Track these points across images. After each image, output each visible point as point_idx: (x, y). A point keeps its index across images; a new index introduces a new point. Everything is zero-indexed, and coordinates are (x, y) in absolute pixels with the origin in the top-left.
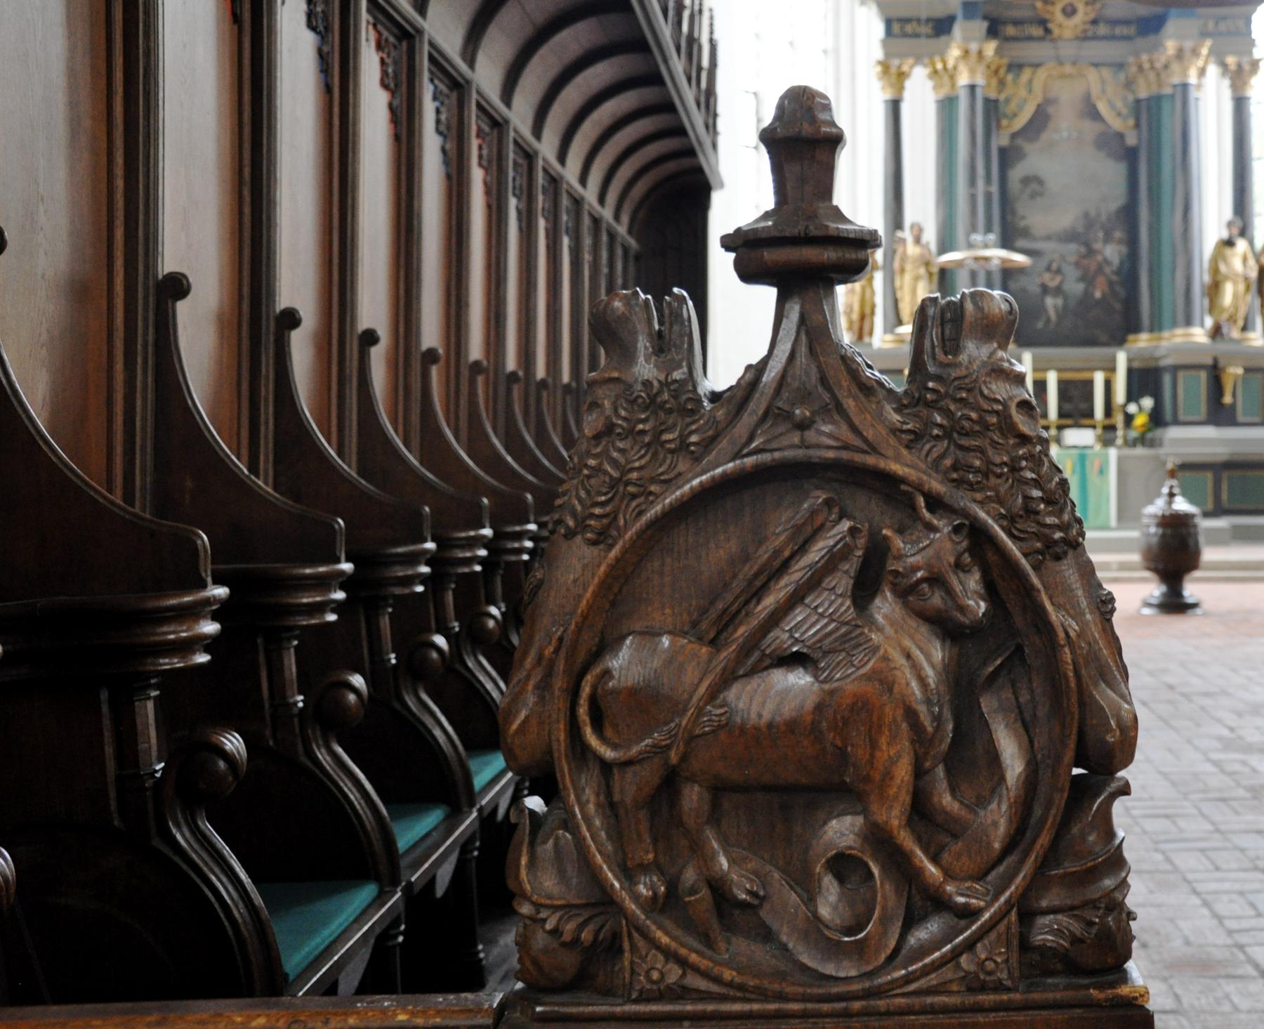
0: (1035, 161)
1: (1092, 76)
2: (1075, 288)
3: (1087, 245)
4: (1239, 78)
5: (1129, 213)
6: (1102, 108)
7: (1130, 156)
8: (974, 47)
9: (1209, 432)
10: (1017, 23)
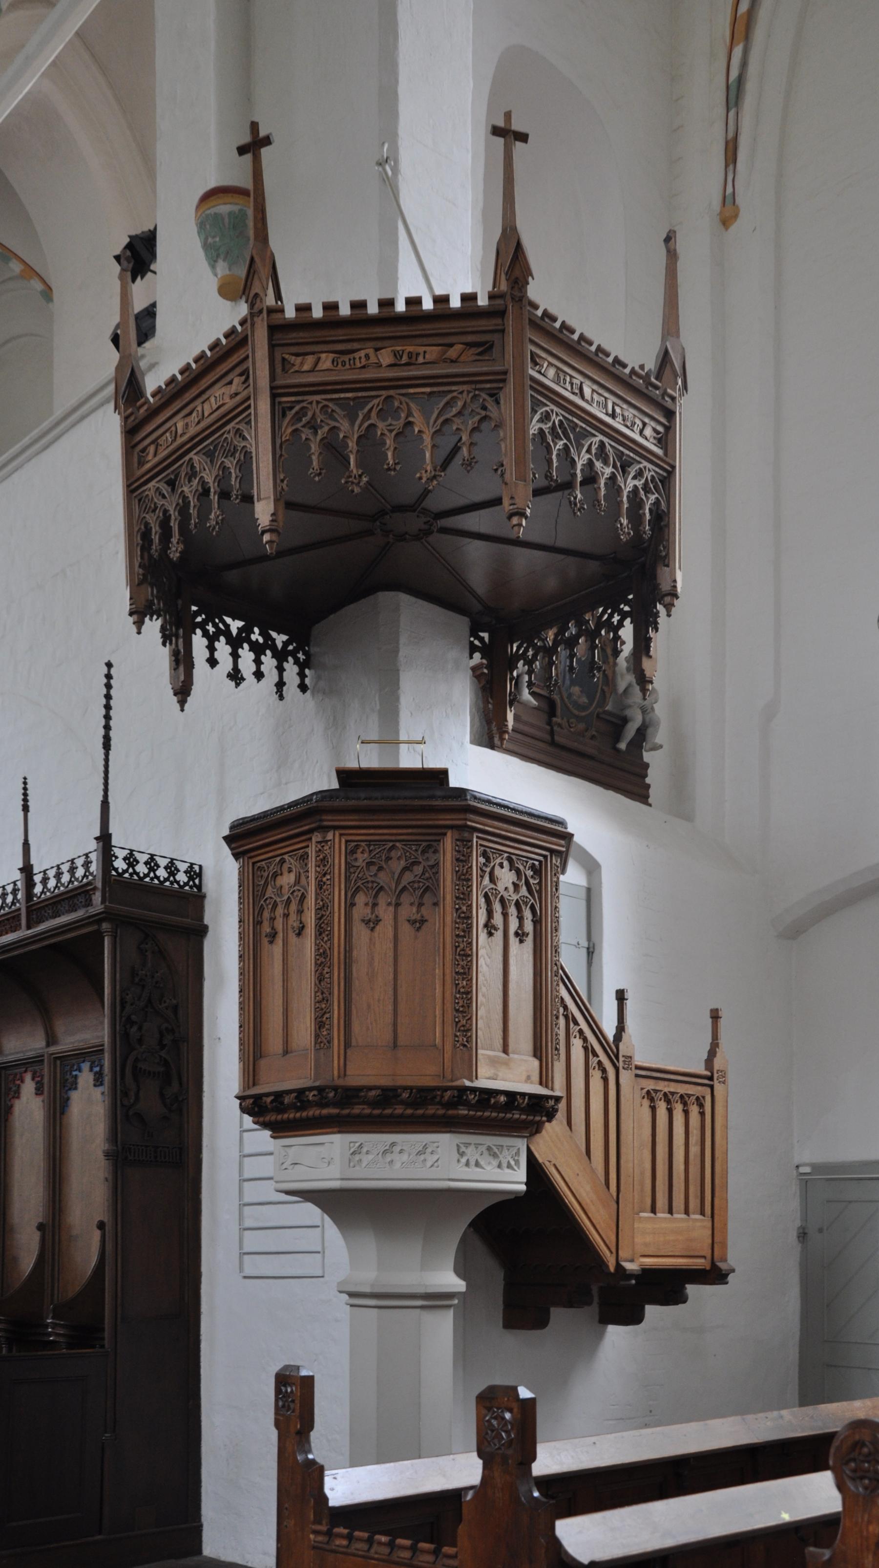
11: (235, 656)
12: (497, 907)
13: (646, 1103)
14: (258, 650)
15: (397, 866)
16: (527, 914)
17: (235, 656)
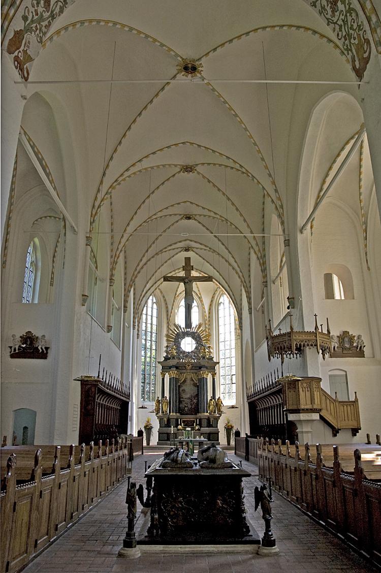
2: (190, 406)
4: (214, 375)
5: (197, 395)
6: (194, 379)
7: (198, 386)
9: (207, 428)
14: (293, 354)
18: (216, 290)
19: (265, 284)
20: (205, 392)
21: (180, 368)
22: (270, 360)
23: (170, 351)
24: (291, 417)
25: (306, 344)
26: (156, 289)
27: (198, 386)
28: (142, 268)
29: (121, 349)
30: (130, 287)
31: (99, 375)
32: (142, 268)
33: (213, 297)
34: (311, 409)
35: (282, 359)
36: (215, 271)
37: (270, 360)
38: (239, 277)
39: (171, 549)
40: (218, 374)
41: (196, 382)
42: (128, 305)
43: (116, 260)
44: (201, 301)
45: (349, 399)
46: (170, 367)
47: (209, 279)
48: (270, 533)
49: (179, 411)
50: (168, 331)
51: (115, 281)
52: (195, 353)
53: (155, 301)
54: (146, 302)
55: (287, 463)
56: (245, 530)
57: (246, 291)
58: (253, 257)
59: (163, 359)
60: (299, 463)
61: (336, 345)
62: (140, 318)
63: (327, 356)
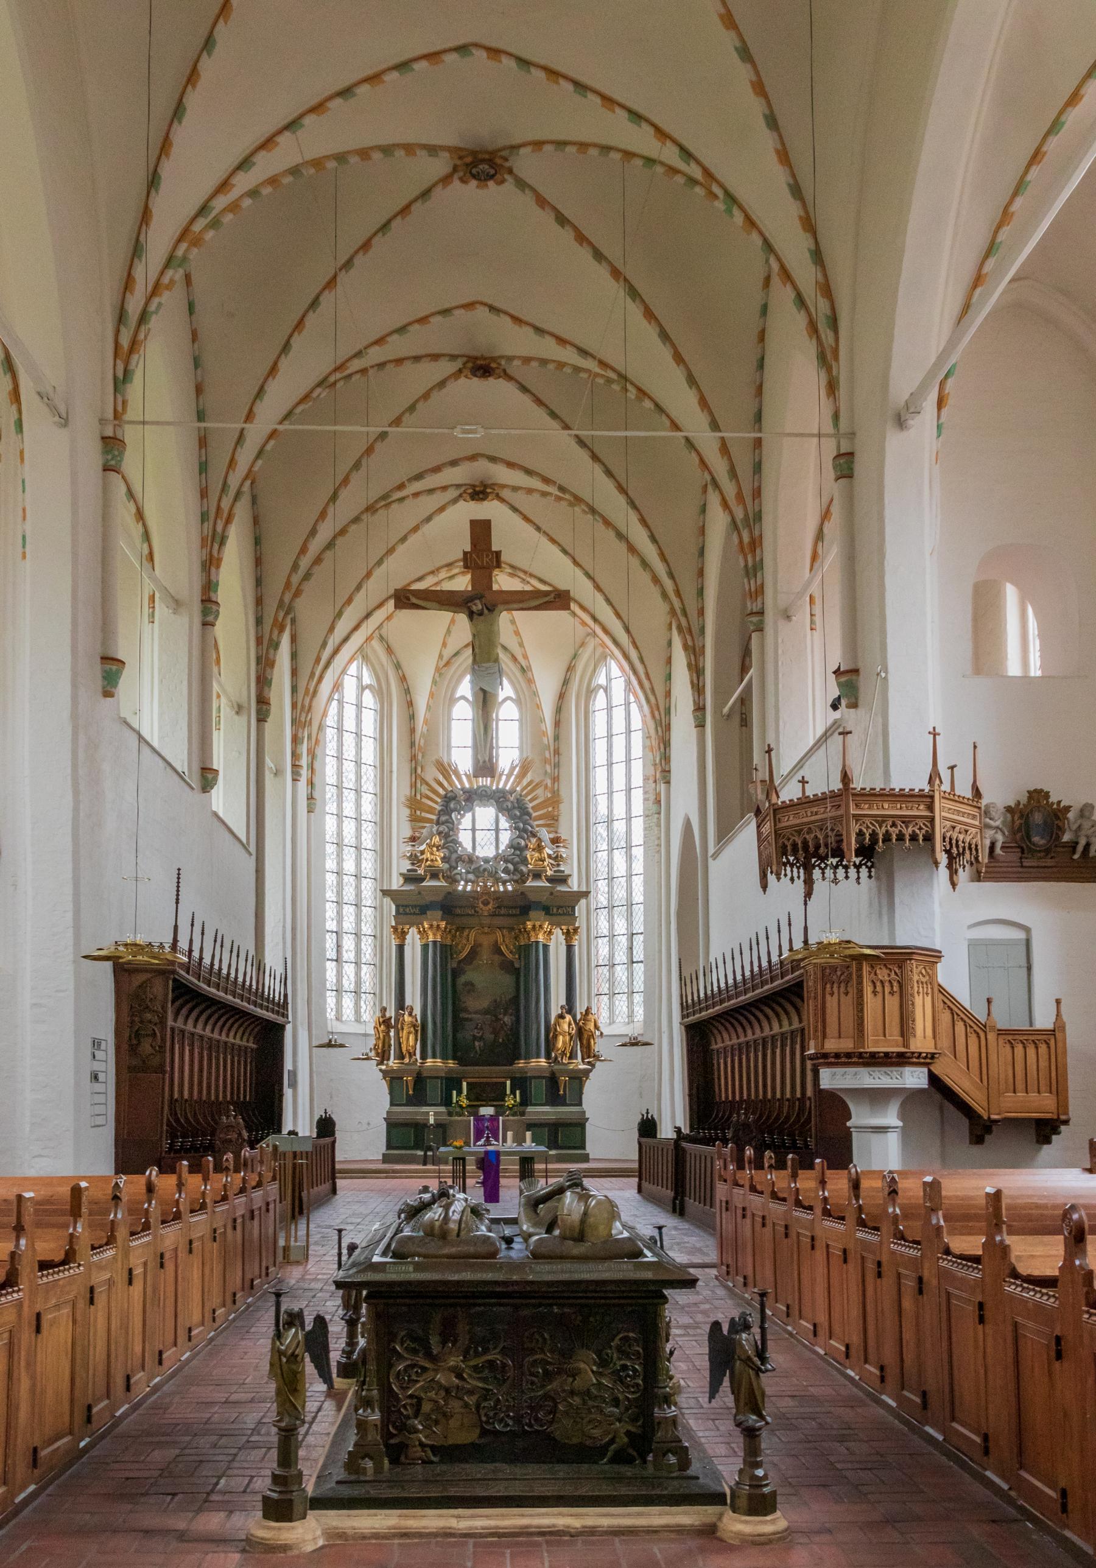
0: (470, 975)
1: (499, 934)
3: (496, 1016)
6: (503, 948)
7: (516, 972)
8: (435, 923)
10: (461, 907)
11: (835, 873)
12: (878, 984)
13: (1008, 1046)
14: (846, 867)
15: (839, 973)
16: (895, 984)
17: (835, 873)
18: (583, 644)
19: (755, 619)
20: (542, 989)
21: (458, 911)
22: (764, 886)
23: (422, 853)
24: (830, 1079)
25: (894, 831)
26: (369, 639)
27: (516, 972)
28: (318, 560)
29: (252, 848)
30: (276, 632)
31: (175, 941)
32: (318, 560)
33: (570, 669)
34: (901, 1055)
35: (809, 883)
36: (579, 573)
37: (764, 886)
38: (665, 595)
39: (424, 1523)
40: (583, 931)
41: (510, 956)
42: (273, 696)
43: (219, 529)
44: (530, 681)
45: (1031, 1025)
46: (423, 910)
47: (558, 600)
48: (760, 1473)
49: (455, 1051)
50: (414, 786)
51: (221, 610)
52: (506, 861)
53: (367, 679)
54: (337, 686)
55: (818, 1233)
56: (672, 1459)
57: (686, 647)
58: (718, 522)
59: (401, 881)
60: (859, 1235)
61: (1000, 839)
62: (317, 742)
63: (963, 875)
